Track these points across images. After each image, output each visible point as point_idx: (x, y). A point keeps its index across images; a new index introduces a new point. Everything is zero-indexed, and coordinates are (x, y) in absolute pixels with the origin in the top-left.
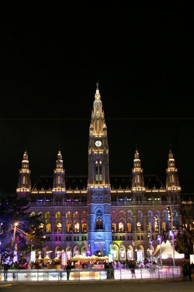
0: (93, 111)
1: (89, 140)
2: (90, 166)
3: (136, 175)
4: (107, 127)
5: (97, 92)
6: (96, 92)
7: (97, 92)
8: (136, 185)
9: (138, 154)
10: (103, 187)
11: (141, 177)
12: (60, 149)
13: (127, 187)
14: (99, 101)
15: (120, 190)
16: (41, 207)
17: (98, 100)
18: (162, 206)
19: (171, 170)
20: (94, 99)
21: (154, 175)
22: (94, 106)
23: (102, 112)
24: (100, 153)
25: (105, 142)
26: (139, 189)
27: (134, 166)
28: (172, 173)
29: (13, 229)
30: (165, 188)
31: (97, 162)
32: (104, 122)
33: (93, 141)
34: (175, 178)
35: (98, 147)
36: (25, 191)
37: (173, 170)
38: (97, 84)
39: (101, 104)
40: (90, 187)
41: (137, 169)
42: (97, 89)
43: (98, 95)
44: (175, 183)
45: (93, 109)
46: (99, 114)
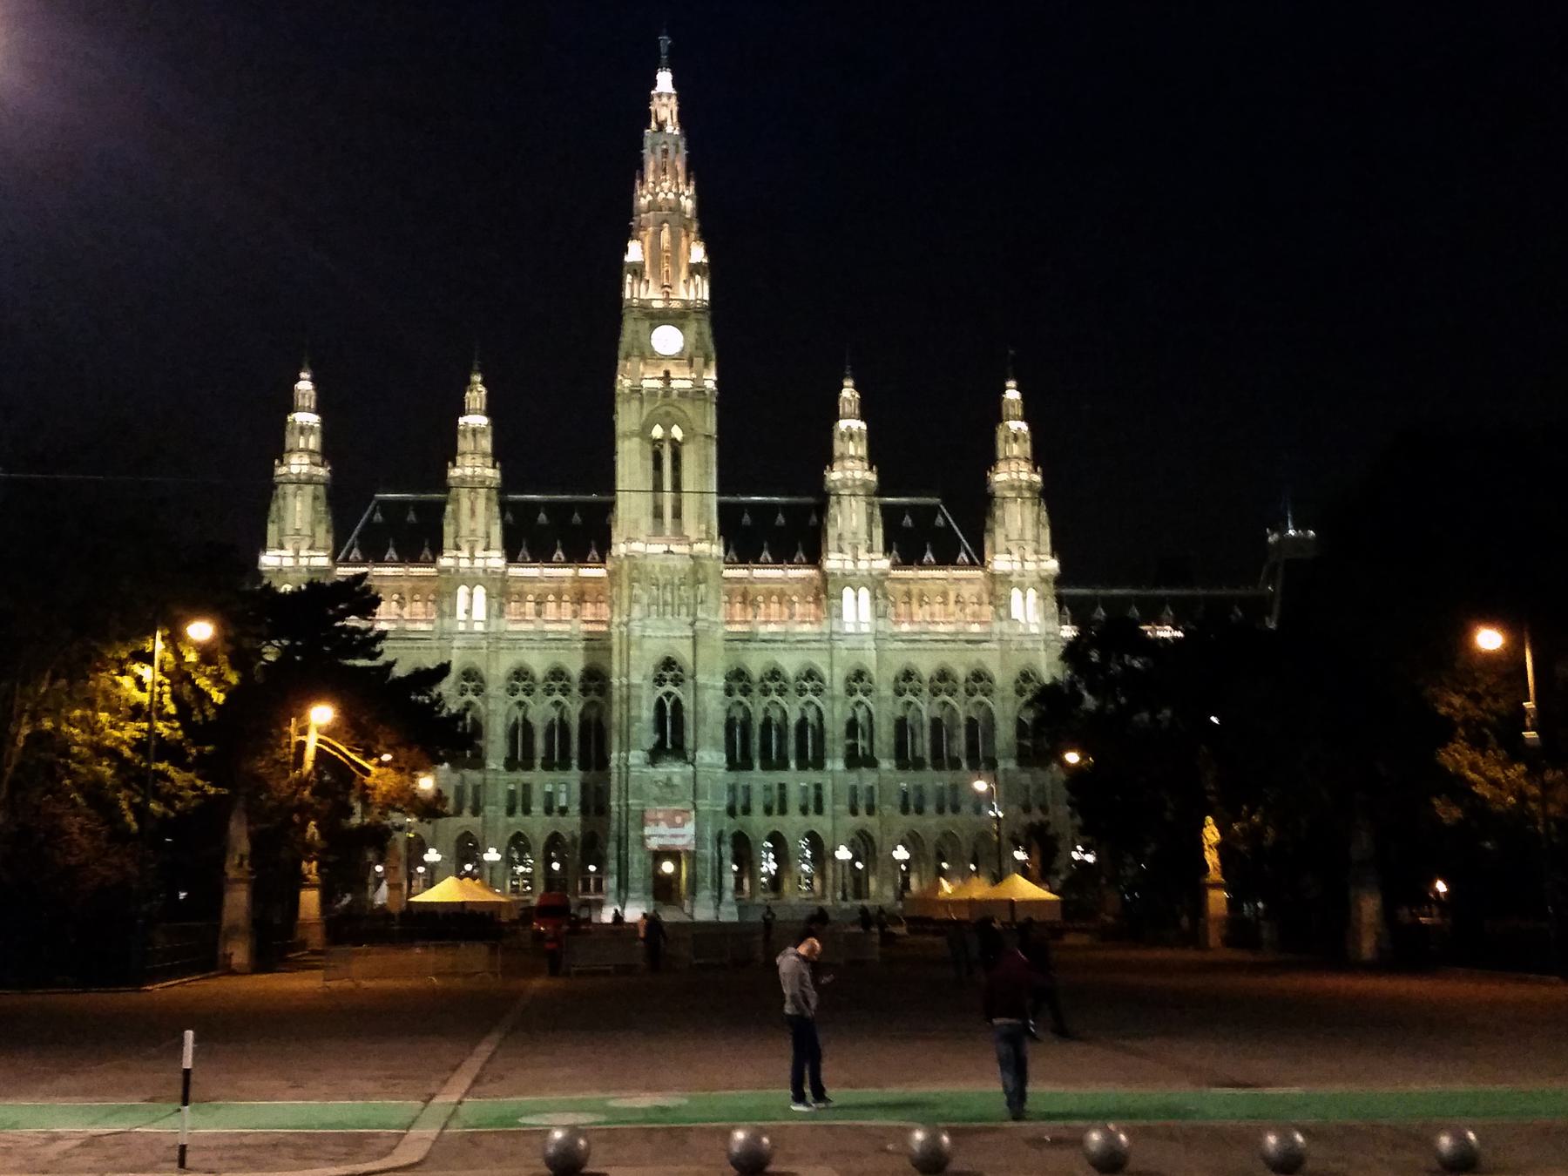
4: (710, 259)
5: (664, 80)
6: (654, 84)
7: (664, 80)
11: (870, 504)
12: (476, 367)
13: (800, 555)
20: (645, 116)
23: (688, 185)
25: (700, 334)
26: (856, 559)
29: (303, 738)
30: (982, 559)
32: (693, 236)
37: (1024, 476)
39: (682, 144)
41: (849, 464)
43: (665, 100)
44: (1029, 534)
45: (640, 165)
46: (671, 196)
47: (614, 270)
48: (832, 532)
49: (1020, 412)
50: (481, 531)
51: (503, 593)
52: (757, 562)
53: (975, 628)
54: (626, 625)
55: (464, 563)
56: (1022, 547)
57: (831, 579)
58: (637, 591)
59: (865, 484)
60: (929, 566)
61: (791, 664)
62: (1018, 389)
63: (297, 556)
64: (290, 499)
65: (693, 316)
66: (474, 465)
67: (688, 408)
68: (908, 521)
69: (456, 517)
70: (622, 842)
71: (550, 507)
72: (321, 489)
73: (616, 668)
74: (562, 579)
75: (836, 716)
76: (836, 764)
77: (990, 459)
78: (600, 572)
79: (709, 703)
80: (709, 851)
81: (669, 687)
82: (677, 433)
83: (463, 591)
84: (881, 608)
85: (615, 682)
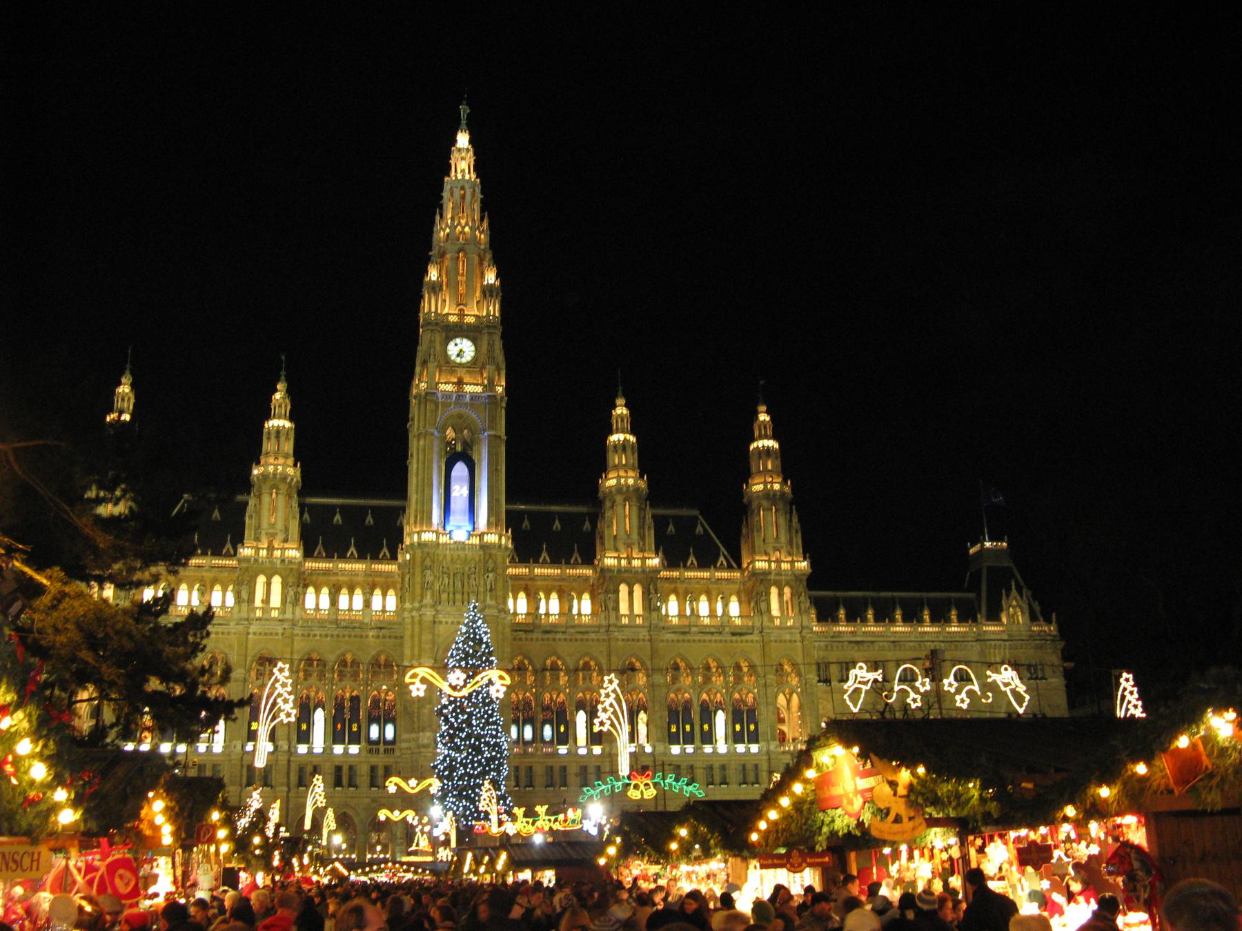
2: (422, 443)
3: (619, 499)
4: (501, 282)
5: (463, 139)
6: (456, 141)
7: (463, 139)
8: (621, 547)
9: (625, 411)
13: (576, 555)
14: (467, 177)
15: (544, 564)
17: (463, 171)
18: (729, 638)
19: (765, 483)
22: (446, 194)
23: (482, 219)
24: (469, 389)
26: (629, 559)
27: (610, 463)
28: (768, 495)
33: (438, 338)
34: (782, 521)
35: (461, 365)
37: (777, 487)
38: (464, 110)
39: (478, 190)
40: (419, 537)
46: (467, 229)
47: (414, 289)
49: (769, 432)
50: (280, 526)
51: (298, 582)
52: (536, 561)
54: (419, 609)
55: (263, 553)
57: (608, 575)
58: (429, 578)
59: (637, 489)
60: (691, 568)
62: (768, 412)
65: (485, 331)
66: (277, 464)
68: (671, 528)
69: (258, 513)
71: (344, 509)
74: (354, 573)
78: (392, 567)
83: (261, 580)
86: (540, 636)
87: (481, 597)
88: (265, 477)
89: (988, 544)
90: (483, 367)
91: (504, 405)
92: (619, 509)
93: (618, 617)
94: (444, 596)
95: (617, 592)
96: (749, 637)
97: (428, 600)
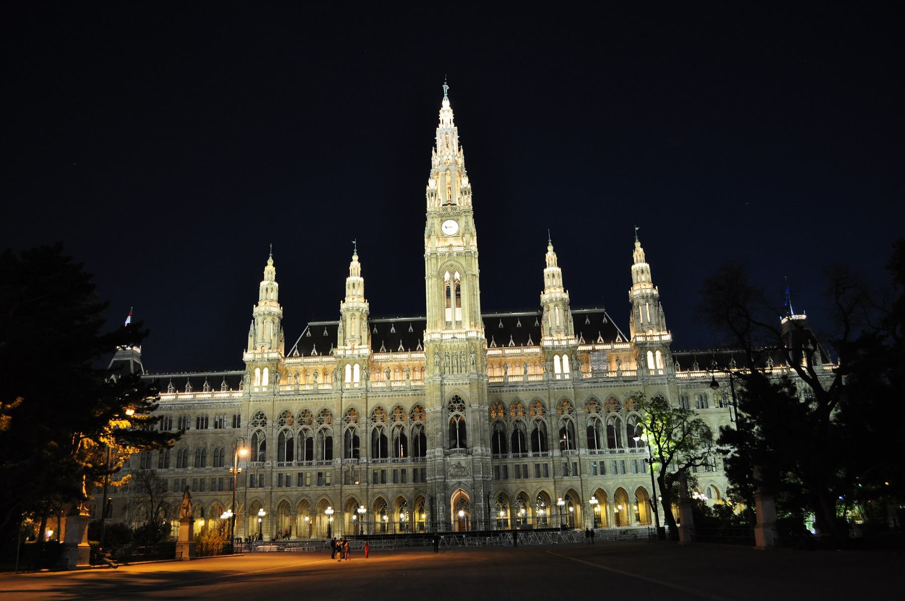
0: (436, 151)
1: (425, 219)
3: (552, 305)
5: (446, 103)
6: (441, 106)
7: (446, 103)
8: (553, 333)
10: (464, 336)
11: (565, 310)
13: (530, 340)
14: (449, 126)
16: (306, 396)
20: (436, 122)
21: (596, 310)
24: (455, 249)
25: (467, 223)
28: (645, 298)
30: (629, 338)
31: (447, 276)
34: (653, 311)
36: (266, 356)
37: (649, 291)
38: (446, 87)
42: (446, 97)
43: (446, 113)
44: (654, 323)
45: (436, 146)
46: (450, 157)
48: (546, 326)
49: (643, 258)
50: (357, 336)
51: (369, 367)
52: (506, 345)
53: (628, 374)
56: (650, 327)
59: (562, 299)
61: (526, 398)
63: (263, 353)
64: (260, 324)
67: (463, 261)
70: (432, 500)
71: (396, 324)
72: (277, 321)
73: (428, 403)
75: (553, 426)
76: (557, 453)
77: (630, 284)
78: (423, 355)
79: (474, 418)
80: (482, 504)
81: (457, 412)
82: (457, 276)
84: (575, 364)
85: (427, 410)
86: (508, 389)
87: (468, 368)
88: (348, 310)
89: (794, 317)
90: (463, 235)
91: (477, 256)
92: (552, 311)
93: (554, 375)
94: (447, 369)
95: (552, 360)
96: (635, 383)
97: (437, 371)
